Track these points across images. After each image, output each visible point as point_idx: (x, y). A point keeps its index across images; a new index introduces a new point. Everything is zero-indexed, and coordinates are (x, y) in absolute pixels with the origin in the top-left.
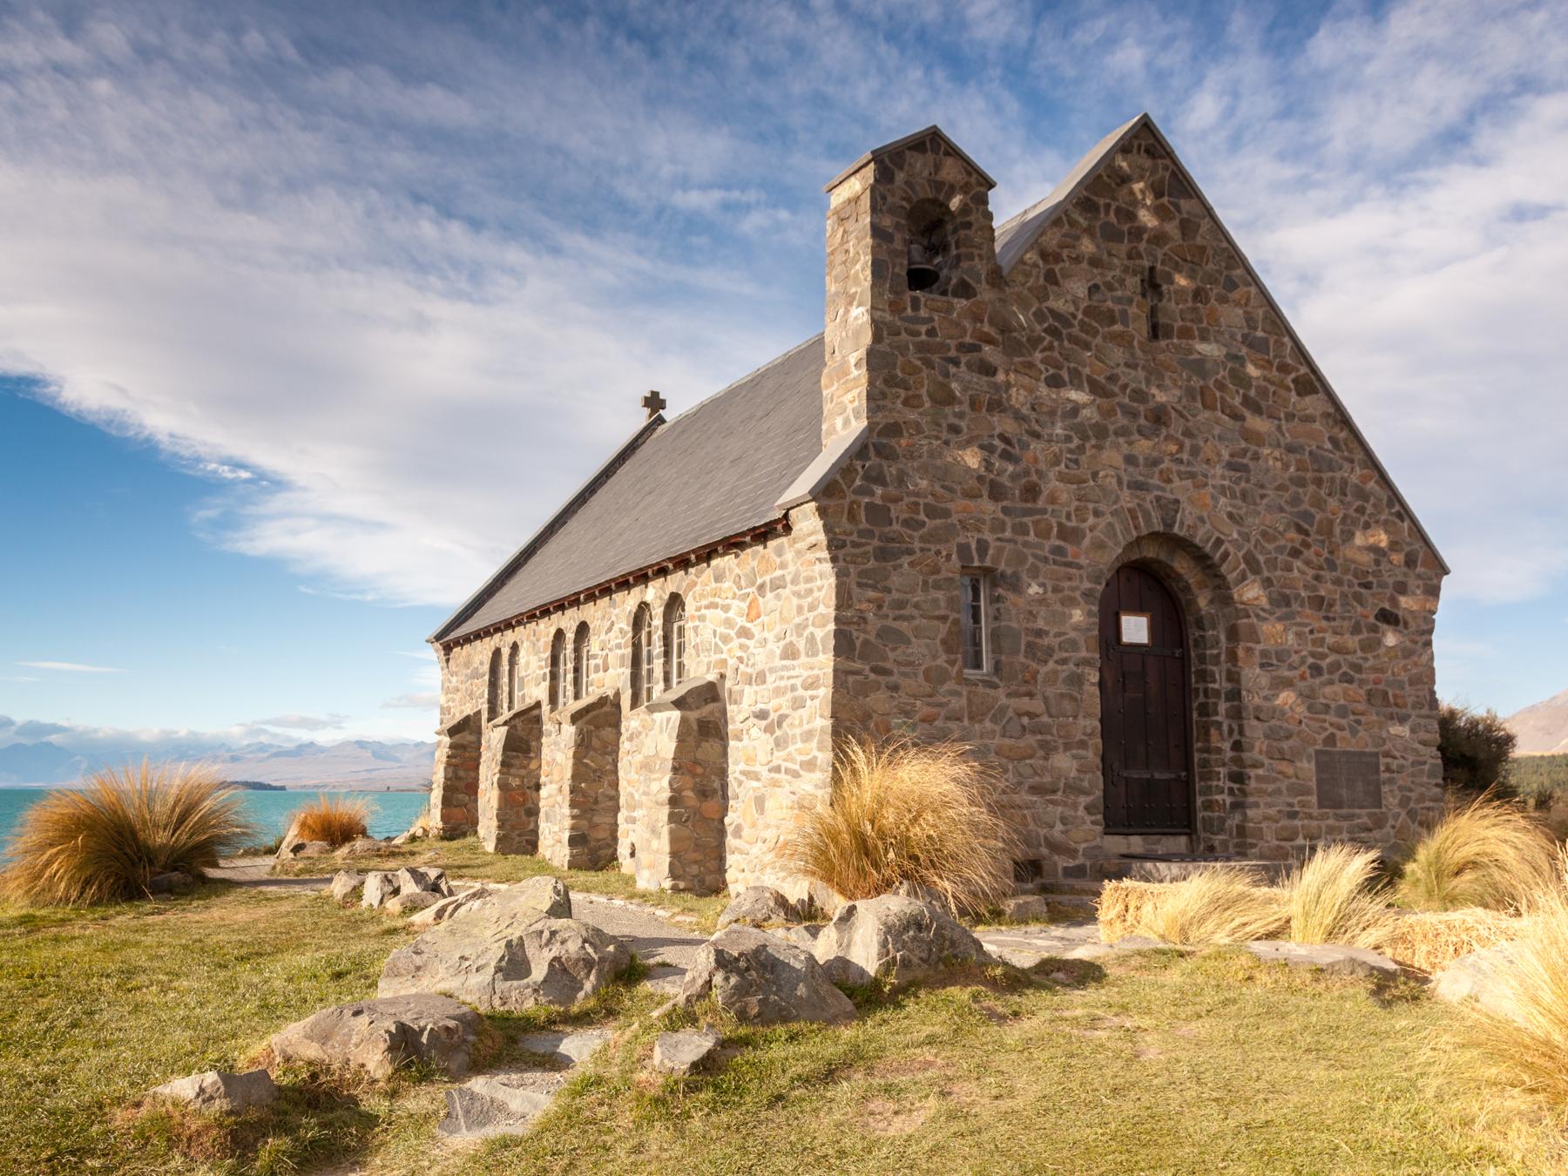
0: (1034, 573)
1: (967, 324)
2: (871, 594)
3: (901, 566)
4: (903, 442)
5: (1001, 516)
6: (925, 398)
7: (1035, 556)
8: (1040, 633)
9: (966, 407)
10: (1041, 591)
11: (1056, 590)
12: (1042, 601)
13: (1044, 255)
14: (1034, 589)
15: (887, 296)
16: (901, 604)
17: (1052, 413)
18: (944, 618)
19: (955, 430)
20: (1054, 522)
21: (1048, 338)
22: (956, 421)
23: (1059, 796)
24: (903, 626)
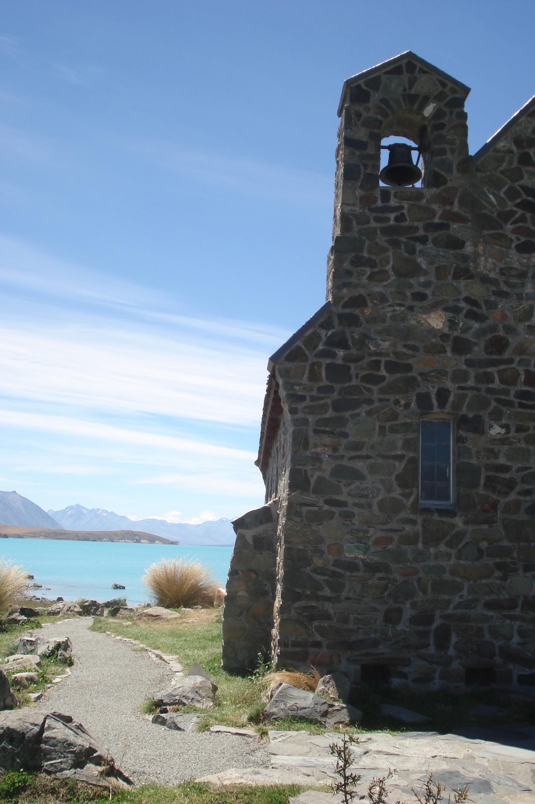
0: (497, 416)
1: (435, 207)
2: (327, 439)
3: (358, 415)
4: (368, 311)
5: (464, 367)
6: (391, 273)
7: (498, 401)
8: (505, 469)
9: (432, 277)
10: (503, 431)
11: (519, 430)
12: (503, 441)
13: (518, 142)
14: (496, 430)
15: (359, 193)
16: (357, 446)
17: (522, 275)
18: (400, 458)
19: (420, 297)
20: (521, 370)
21: (520, 212)
22: (421, 290)
23: (517, 612)
24: (360, 465)
